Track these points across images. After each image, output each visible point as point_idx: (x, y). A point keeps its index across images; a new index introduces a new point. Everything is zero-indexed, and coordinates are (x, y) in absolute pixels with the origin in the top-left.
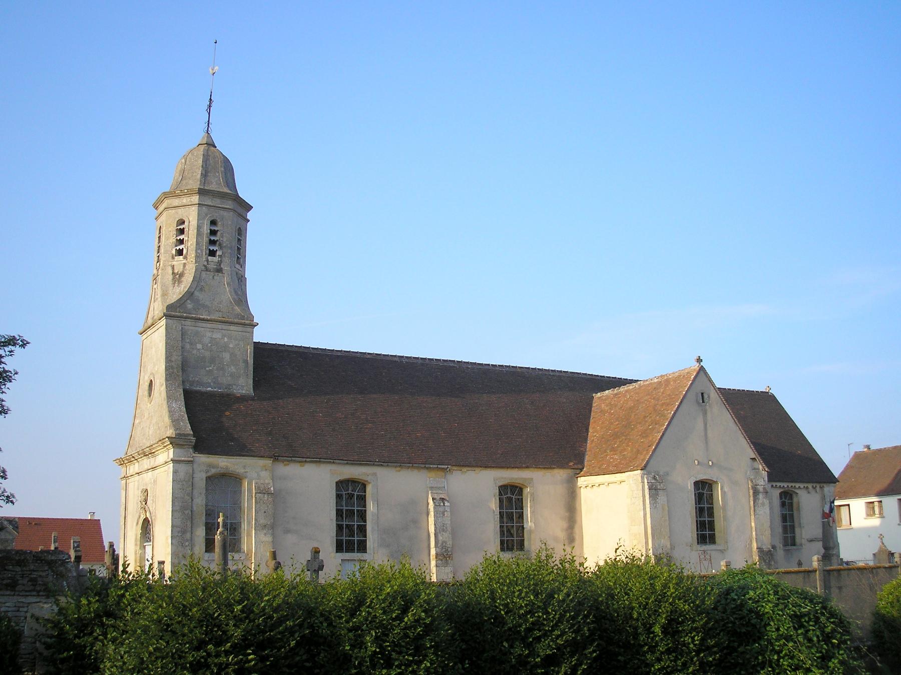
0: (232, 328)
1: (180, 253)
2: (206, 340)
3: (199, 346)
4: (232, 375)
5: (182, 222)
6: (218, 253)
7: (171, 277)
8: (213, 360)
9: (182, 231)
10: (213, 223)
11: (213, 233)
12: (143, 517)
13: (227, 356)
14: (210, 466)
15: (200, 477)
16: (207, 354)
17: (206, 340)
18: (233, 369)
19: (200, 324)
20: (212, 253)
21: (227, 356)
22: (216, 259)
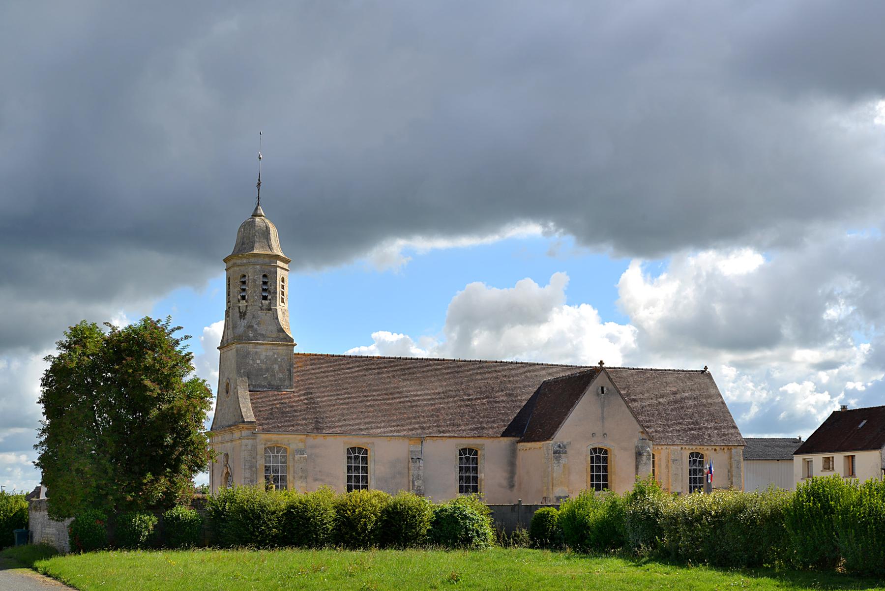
0: (280, 348)
1: (243, 298)
2: (263, 357)
3: (258, 361)
4: (280, 379)
5: (244, 276)
6: (269, 297)
7: (238, 315)
8: (267, 370)
9: (244, 283)
10: (265, 276)
11: (265, 283)
12: (225, 471)
13: (276, 367)
14: (267, 441)
15: (261, 448)
16: (264, 366)
17: (263, 357)
18: (281, 375)
19: (258, 346)
20: (265, 298)
21: (276, 367)
22: (267, 302)
